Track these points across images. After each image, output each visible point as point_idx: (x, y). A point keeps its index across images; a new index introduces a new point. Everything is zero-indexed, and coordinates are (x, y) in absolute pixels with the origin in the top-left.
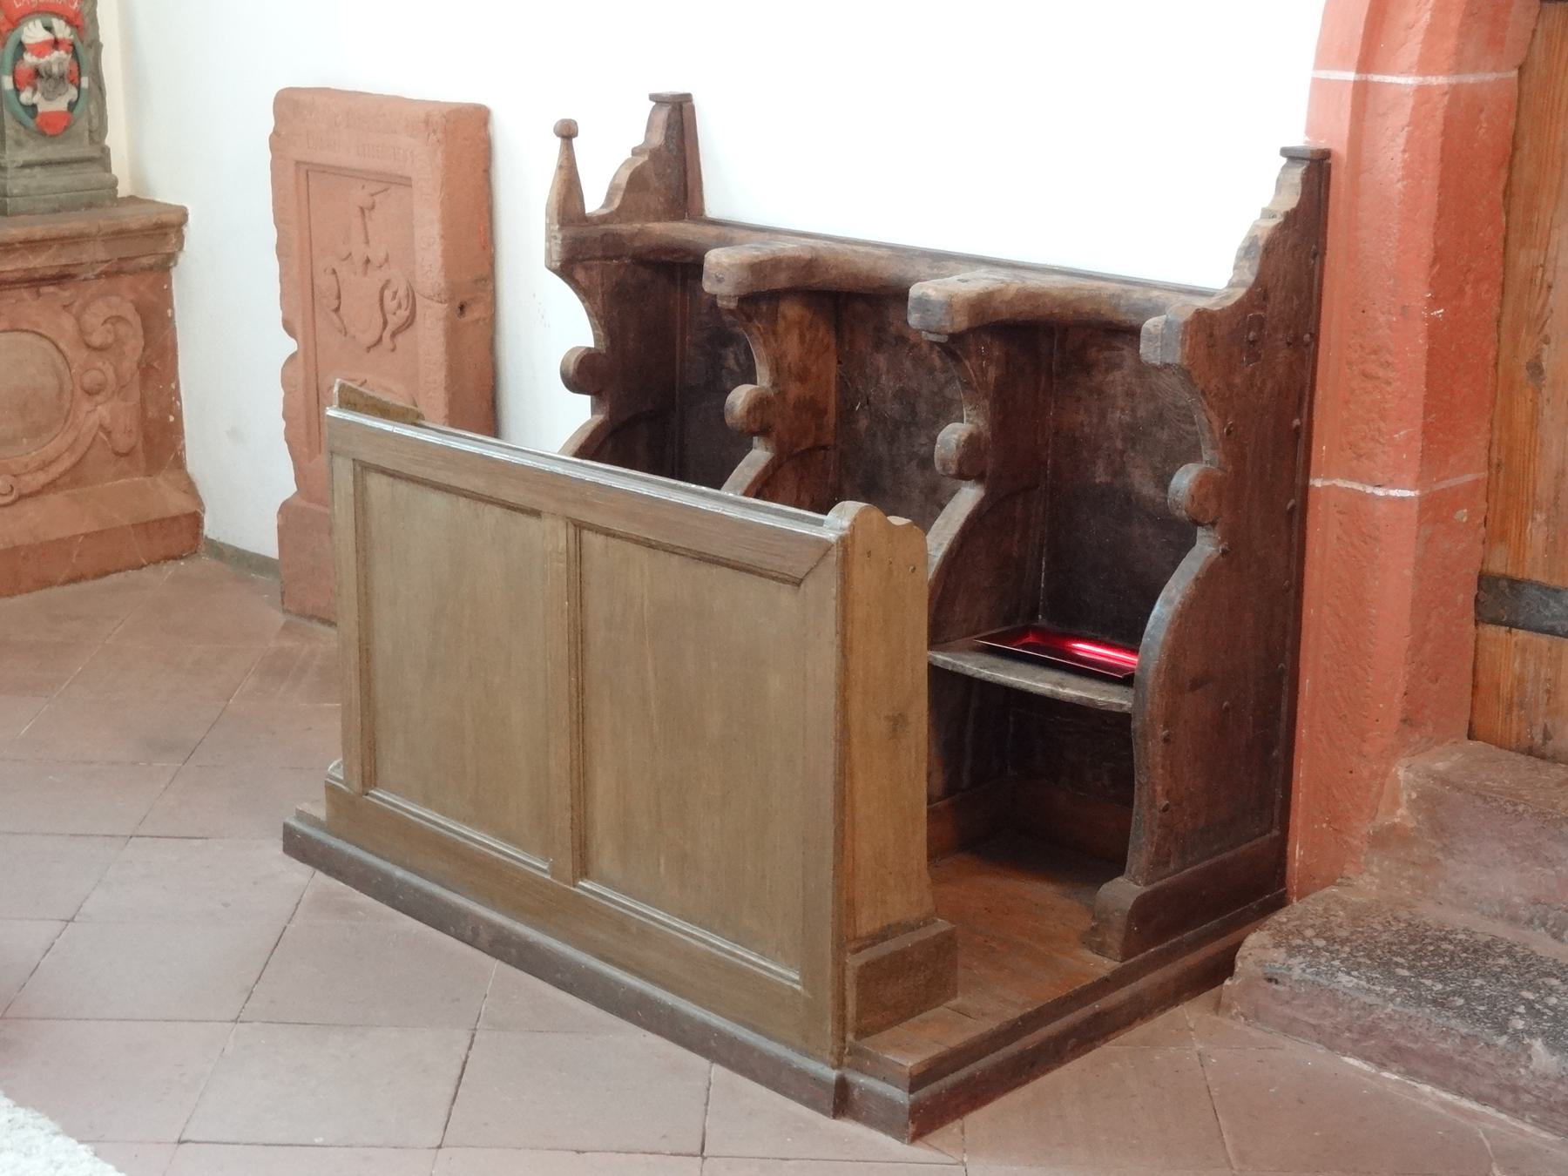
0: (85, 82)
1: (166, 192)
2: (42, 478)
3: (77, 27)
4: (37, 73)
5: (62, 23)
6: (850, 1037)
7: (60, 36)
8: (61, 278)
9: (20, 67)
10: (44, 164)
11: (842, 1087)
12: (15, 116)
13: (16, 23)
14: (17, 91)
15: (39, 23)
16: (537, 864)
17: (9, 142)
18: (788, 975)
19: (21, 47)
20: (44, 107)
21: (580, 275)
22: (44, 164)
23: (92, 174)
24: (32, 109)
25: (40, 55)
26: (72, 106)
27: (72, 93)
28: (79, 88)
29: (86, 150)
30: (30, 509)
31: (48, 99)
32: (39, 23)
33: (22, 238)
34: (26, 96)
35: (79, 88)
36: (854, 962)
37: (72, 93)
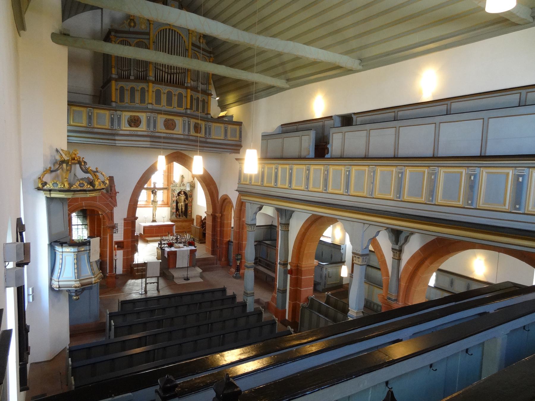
8: (189, 221)
18: (198, 240)
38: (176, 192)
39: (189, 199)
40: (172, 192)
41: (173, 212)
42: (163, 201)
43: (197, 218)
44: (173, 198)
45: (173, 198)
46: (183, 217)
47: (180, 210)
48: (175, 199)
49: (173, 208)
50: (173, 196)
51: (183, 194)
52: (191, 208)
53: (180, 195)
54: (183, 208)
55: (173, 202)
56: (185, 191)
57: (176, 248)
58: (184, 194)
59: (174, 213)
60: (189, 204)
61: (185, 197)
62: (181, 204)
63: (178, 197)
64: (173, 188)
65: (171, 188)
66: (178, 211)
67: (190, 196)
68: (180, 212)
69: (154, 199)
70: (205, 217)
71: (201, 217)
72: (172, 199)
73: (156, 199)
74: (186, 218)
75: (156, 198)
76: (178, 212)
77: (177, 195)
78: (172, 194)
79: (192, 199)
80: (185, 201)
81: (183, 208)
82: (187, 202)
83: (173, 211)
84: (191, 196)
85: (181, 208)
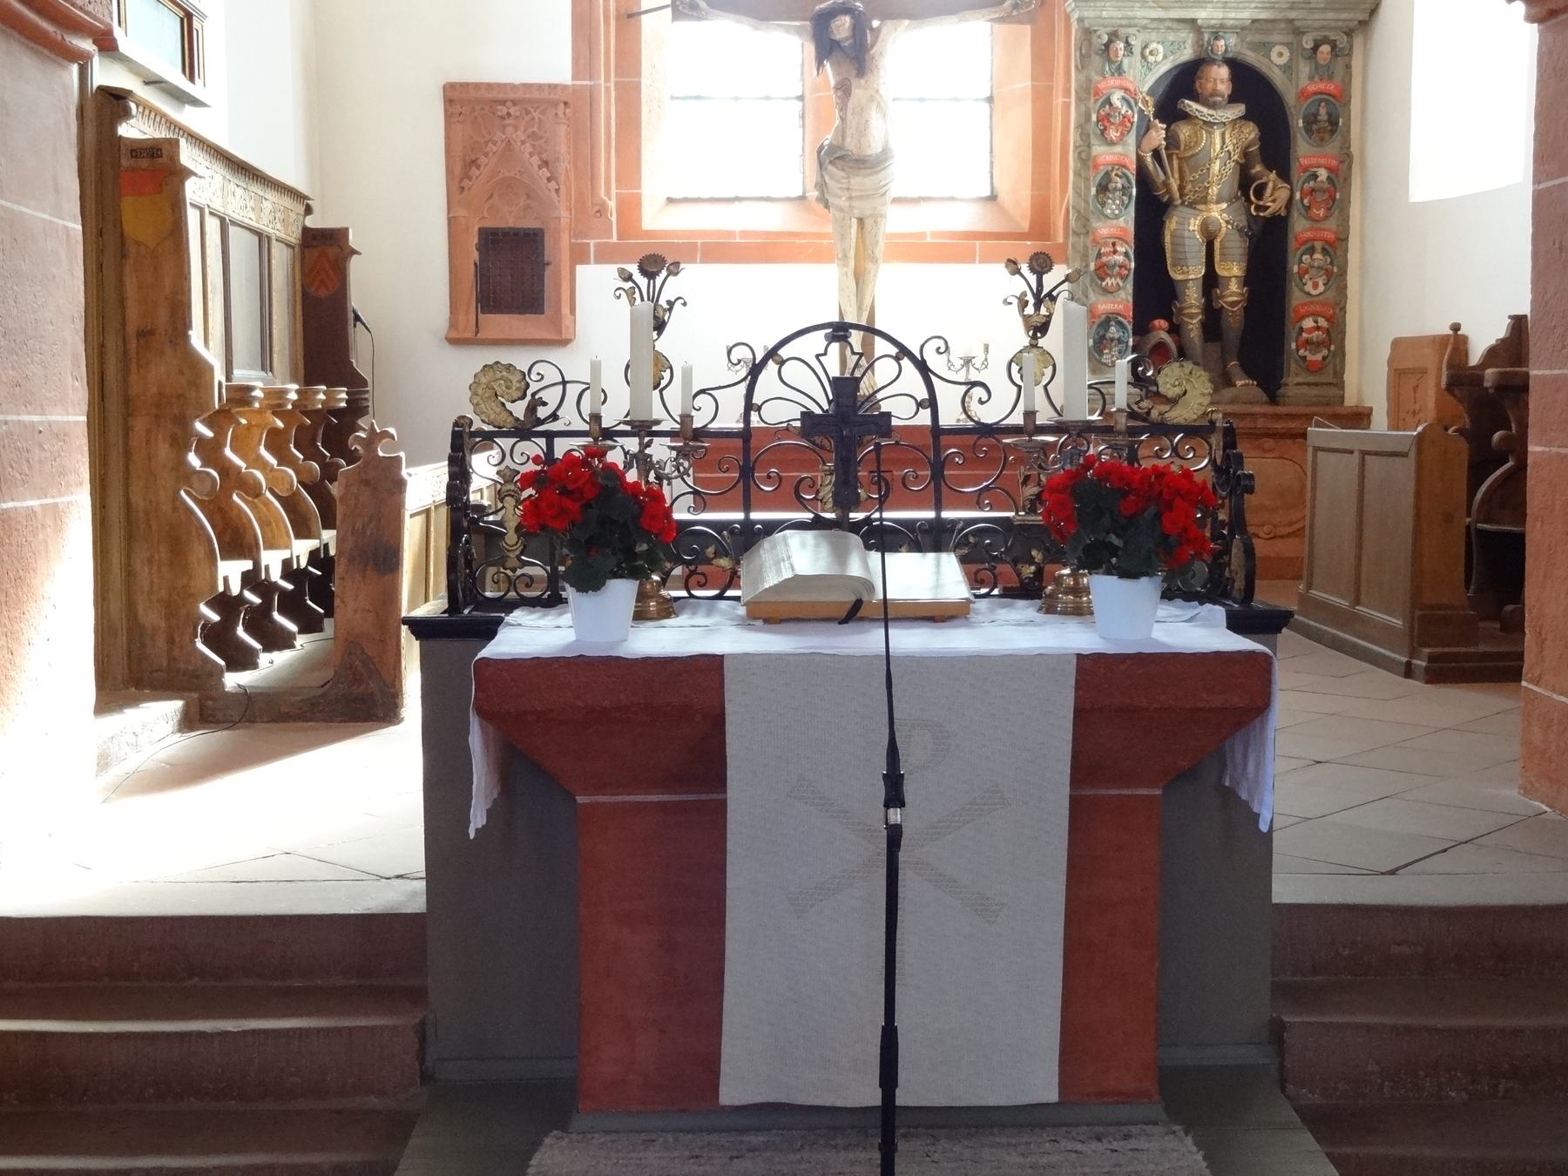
0: (1332, 348)
1: (1368, 404)
2: (1288, 530)
3: (1332, 322)
4: (1307, 342)
5: (1323, 320)
6: (1415, 645)
7: (1319, 324)
9: (1301, 339)
10: (1308, 384)
11: (1409, 664)
12: (1296, 361)
13: (1303, 317)
14: (1298, 350)
15: (1311, 319)
16: (1344, 603)
17: (1292, 373)
18: (1398, 622)
19: (1301, 330)
20: (1310, 357)
21: (1457, 392)
22: (1308, 384)
23: (1333, 391)
24: (1304, 358)
25: (1309, 334)
26: (1324, 358)
27: (1325, 352)
28: (1329, 349)
29: (1330, 379)
30: (1279, 544)
31: (1313, 354)
32: (1311, 319)
33: (1285, 413)
34: (1302, 352)
35: (1329, 349)
36: (1418, 613)
37: (1325, 352)
38: (1132, 65)
39: (1304, 150)
40: (1084, 59)
41: (1105, 324)
42: (993, 197)
43: (1401, 375)
44: (1099, 149)
45: (1099, 149)
46: (1228, 393)
47: (1193, 297)
48: (1122, 152)
49: (1102, 271)
50: (1101, 121)
51: (1224, 88)
52: (1336, 276)
53: (1185, 116)
54: (1232, 270)
55: (1103, 188)
56: (1251, 58)
57: (767, 613)
58: (1233, 99)
59: (1113, 331)
60: (1299, 226)
61: (1251, 132)
62: (1194, 225)
63: (1158, 135)
64: (1089, 14)
65: (1075, 16)
66: (1168, 316)
67: (1311, 120)
68: (1193, 326)
69: (842, 132)
70: (1518, 323)
71: (1456, 342)
72: (1086, 160)
73: (863, 130)
74: (1273, 399)
75: (862, 111)
76: (1163, 323)
77: (1150, 111)
78: (1087, 91)
79: (1346, 157)
80: (1246, 184)
81: (1220, 270)
82: (1283, 194)
83: (1105, 306)
84: (1333, 122)
85: (1197, 271)
